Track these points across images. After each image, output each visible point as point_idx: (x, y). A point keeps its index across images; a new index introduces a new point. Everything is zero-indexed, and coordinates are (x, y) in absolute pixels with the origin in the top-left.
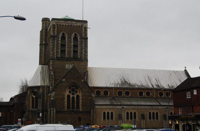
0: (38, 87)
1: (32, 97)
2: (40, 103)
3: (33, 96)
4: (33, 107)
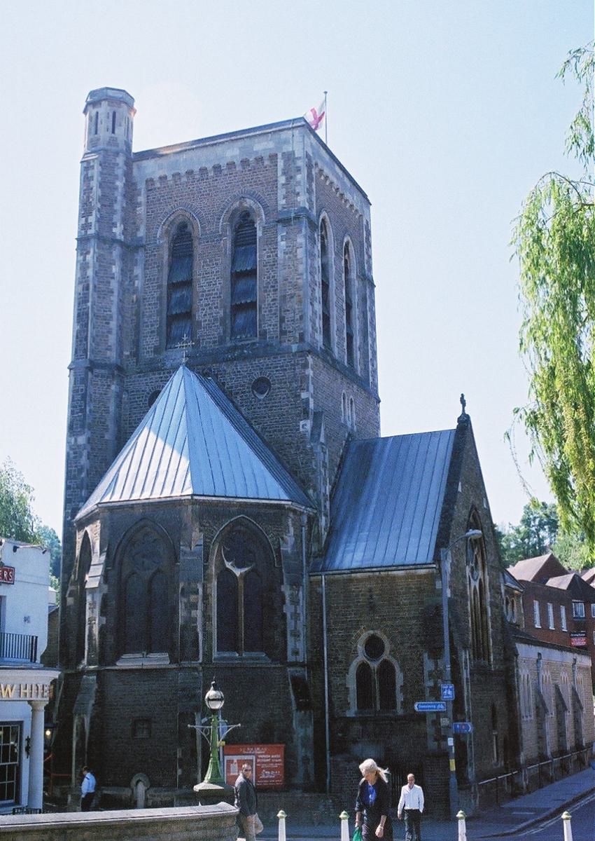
0: (274, 513)
1: (224, 574)
3: (228, 565)
4: (228, 640)
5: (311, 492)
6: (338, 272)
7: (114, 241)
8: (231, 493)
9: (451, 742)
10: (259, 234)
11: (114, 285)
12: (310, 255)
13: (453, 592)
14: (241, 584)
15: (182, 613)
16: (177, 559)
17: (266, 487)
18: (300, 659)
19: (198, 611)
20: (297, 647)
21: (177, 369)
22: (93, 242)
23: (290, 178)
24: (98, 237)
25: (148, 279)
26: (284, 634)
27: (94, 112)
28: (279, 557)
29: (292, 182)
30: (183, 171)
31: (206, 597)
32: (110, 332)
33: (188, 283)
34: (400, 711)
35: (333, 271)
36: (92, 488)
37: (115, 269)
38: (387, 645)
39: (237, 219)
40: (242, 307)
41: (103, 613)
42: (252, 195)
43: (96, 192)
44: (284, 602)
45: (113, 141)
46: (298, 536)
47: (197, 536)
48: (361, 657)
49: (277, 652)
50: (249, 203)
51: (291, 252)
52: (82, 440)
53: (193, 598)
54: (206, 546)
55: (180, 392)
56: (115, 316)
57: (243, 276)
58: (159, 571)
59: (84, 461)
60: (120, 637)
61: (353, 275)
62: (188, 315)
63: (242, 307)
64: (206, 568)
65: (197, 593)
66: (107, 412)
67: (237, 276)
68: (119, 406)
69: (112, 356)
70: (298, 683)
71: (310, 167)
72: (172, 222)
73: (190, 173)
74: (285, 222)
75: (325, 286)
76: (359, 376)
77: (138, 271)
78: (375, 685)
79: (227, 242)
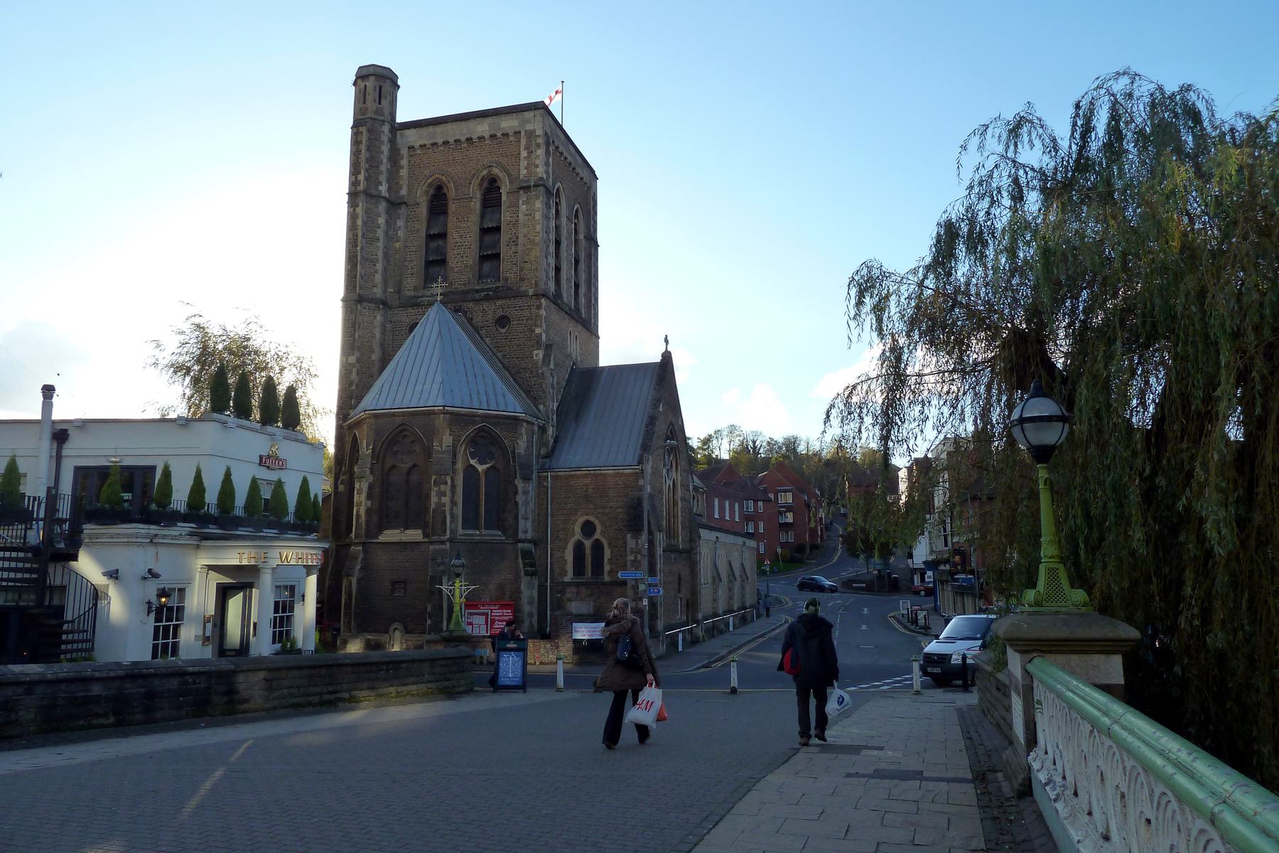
1: (470, 470)
2: (526, 503)
3: (473, 462)
4: (470, 520)
5: (541, 407)
6: (569, 233)
7: (379, 197)
8: (476, 405)
9: (645, 602)
10: (504, 198)
11: (380, 233)
12: (547, 218)
13: (653, 488)
14: (483, 478)
15: (434, 499)
16: (430, 456)
17: (503, 399)
18: (529, 536)
19: (446, 497)
20: (526, 528)
21: (431, 304)
22: (362, 197)
23: (530, 153)
24: (366, 192)
25: (410, 231)
26: (516, 518)
27: (362, 84)
28: (514, 458)
29: (533, 156)
30: (440, 141)
31: (453, 486)
32: (376, 272)
33: (443, 236)
34: (607, 578)
35: (564, 233)
36: (360, 398)
37: (381, 221)
38: (599, 528)
39: (485, 185)
40: (490, 257)
41: (369, 497)
42: (499, 165)
43: (364, 154)
44: (516, 493)
45: (379, 111)
46: (530, 442)
47: (447, 440)
48: (578, 535)
49: (511, 531)
50: (496, 171)
51: (530, 215)
52: (352, 359)
53: (443, 487)
54: (454, 446)
55: (435, 324)
56: (381, 259)
57: (490, 232)
58: (414, 466)
59: (354, 376)
60: (383, 517)
61: (581, 236)
62: (443, 262)
63: (490, 257)
64: (454, 463)
65: (446, 483)
66: (374, 337)
67: (484, 231)
68: (383, 332)
69: (378, 292)
70: (526, 554)
71: (547, 144)
72: (430, 185)
73: (446, 143)
74: (527, 189)
75: (558, 243)
76: (586, 319)
77: (400, 223)
78: (589, 561)
79: (476, 205)
